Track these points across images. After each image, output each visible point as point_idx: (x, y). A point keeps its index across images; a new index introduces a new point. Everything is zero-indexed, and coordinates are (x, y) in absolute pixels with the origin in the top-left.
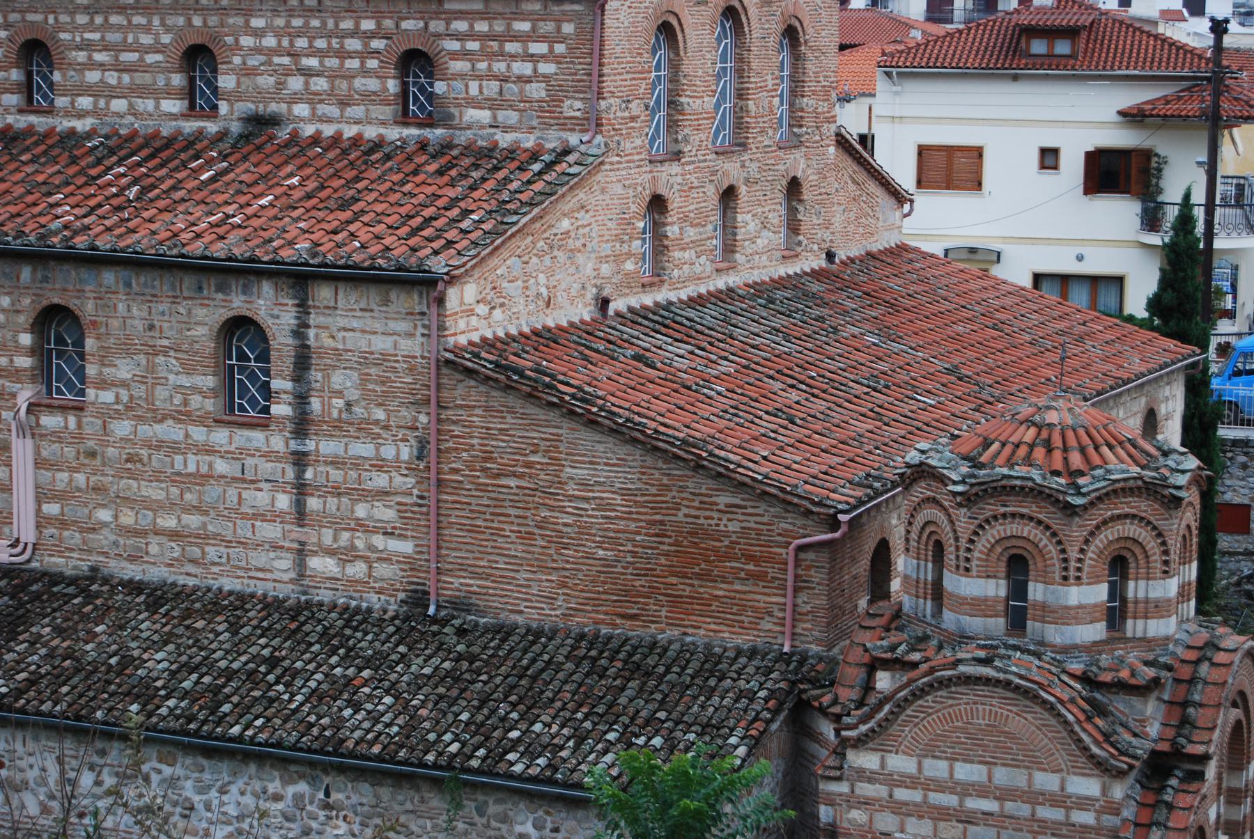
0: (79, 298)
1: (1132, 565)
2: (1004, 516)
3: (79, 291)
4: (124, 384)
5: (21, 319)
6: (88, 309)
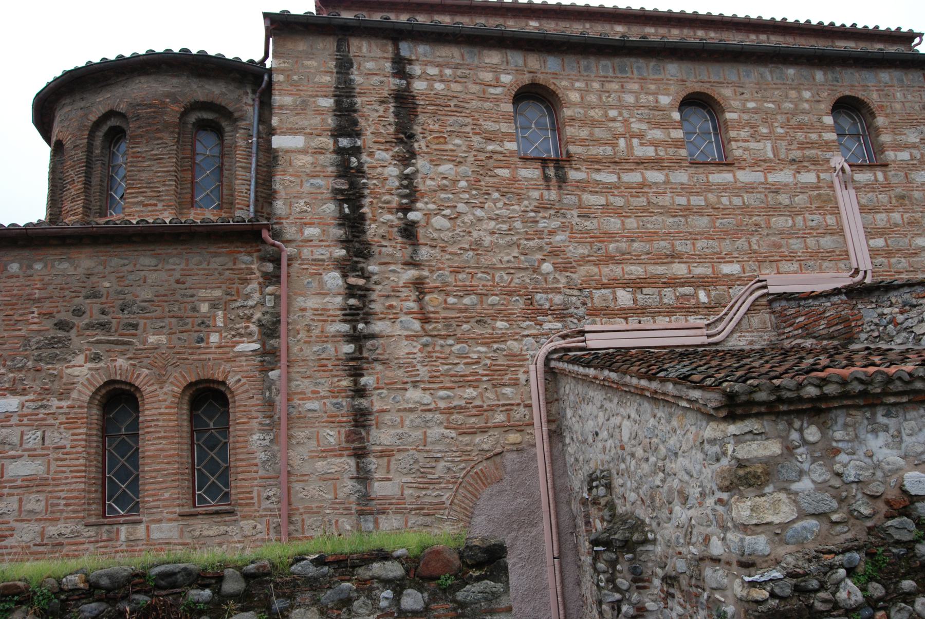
0: (865, 91)
3: (863, 86)
4: (914, 146)
5: (823, 106)
6: (873, 98)
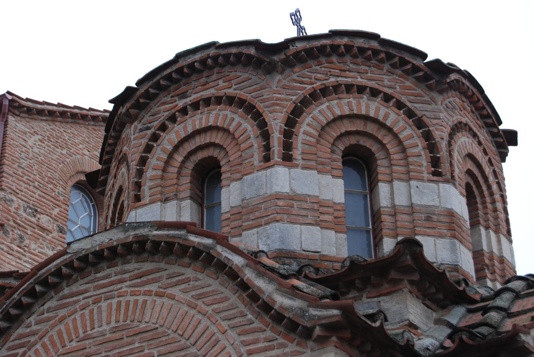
1: (379, 155)
2: (184, 111)
